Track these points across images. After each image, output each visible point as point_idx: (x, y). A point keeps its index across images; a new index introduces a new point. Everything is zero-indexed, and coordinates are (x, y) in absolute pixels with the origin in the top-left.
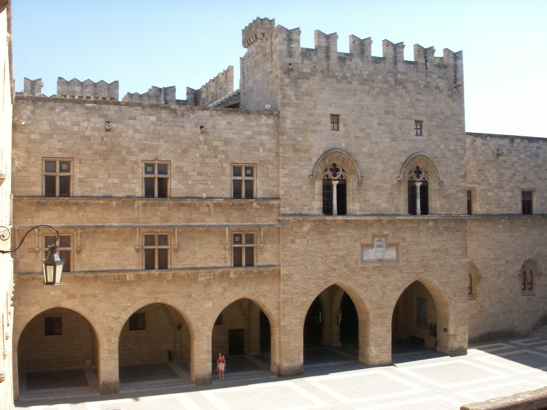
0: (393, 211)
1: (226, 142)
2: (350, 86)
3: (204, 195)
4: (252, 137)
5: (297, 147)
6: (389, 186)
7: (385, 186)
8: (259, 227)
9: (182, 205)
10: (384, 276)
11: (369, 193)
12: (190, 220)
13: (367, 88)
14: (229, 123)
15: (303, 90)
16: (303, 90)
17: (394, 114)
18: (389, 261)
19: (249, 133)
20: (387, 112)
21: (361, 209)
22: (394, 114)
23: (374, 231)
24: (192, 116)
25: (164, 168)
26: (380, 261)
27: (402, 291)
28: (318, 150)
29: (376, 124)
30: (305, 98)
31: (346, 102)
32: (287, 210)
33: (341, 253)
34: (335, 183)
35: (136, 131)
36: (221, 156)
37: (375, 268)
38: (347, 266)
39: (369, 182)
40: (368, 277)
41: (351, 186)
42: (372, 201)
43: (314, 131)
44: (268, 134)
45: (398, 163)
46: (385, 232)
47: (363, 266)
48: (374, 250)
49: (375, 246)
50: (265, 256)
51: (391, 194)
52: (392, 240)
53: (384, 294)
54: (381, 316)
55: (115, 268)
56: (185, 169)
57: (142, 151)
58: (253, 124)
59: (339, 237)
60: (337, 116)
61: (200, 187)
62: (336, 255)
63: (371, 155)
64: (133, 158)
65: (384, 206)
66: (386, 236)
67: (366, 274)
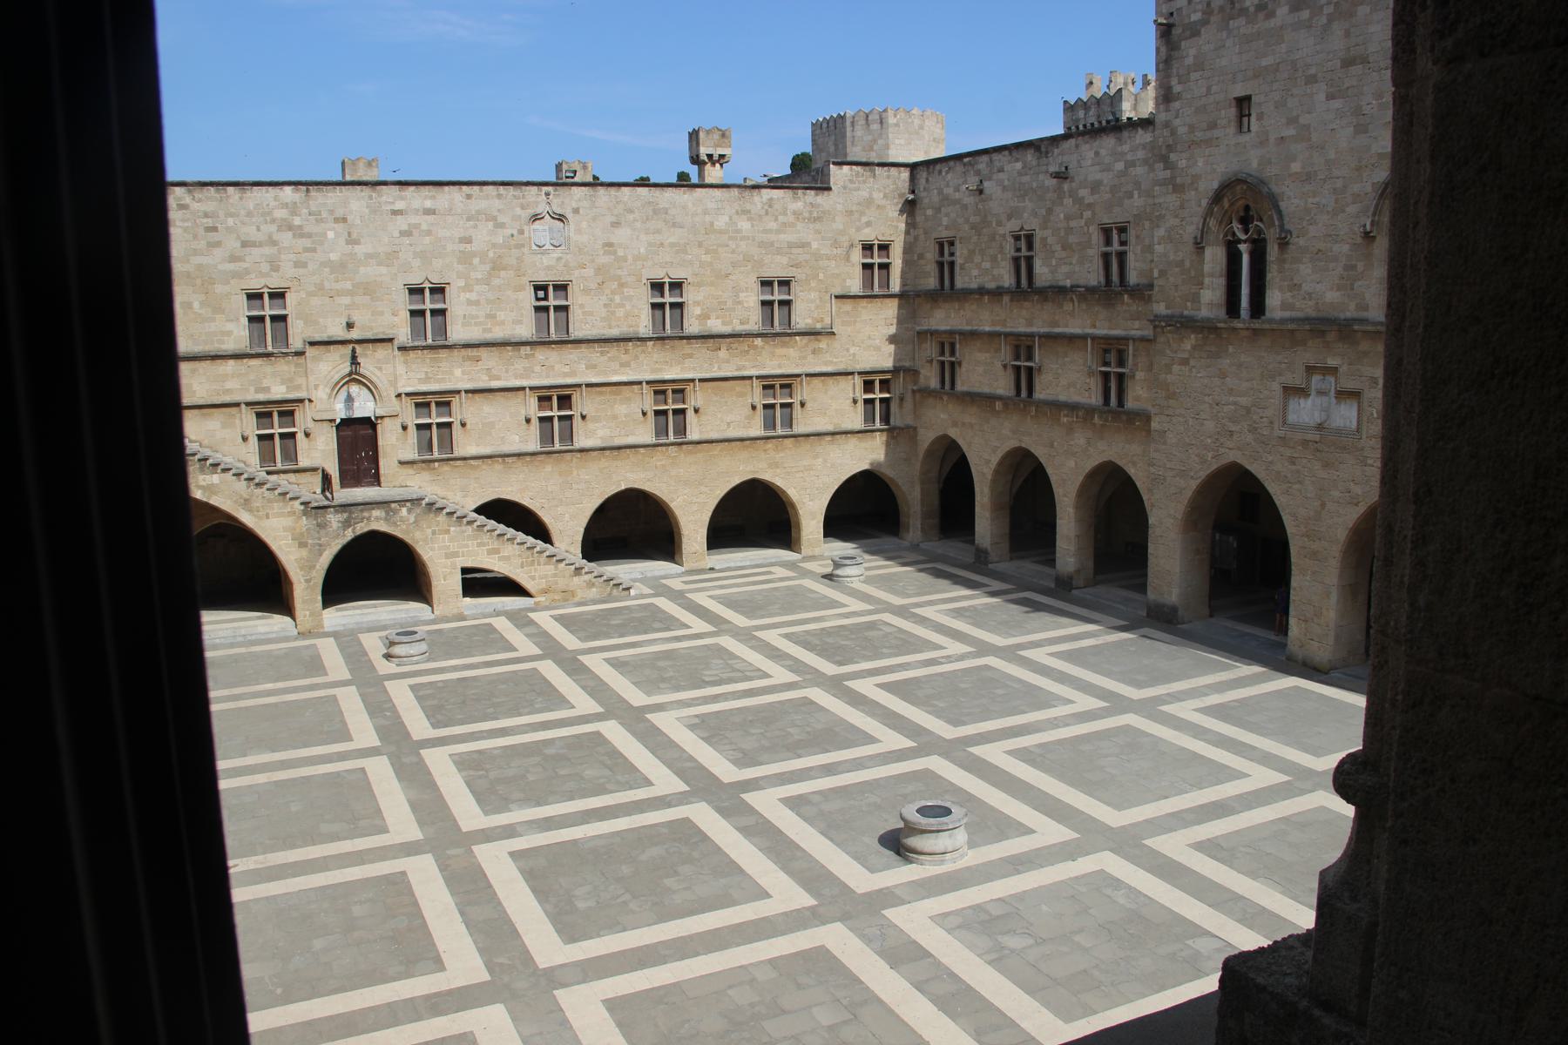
0: (1351, 312)
1: (1095, 187)
2: (1272, 23)
3: (1068, 283)
4: (1124, 173)
5: (1179, 180)
6: (1346, 248)
7: (1336, 248)
8: (1126, 339)
9: (1046, 300)
10: (1326, 465)
11: (1302, 267)
12: (1056, 325)
13: (1305, 14)
14: (1097, 154)
15: (1189, 61)
16: (1189, 61)
17: (1364, 60)
18: (1339, 432)
19: (1120, 166)
20: (1348, 63)
21: (1285, 306)
22: (1364, 60)
23: (1308, 355)
24: (1056, 151)
25: (1030, 239)
26: (1320, 427)
27: (1362, 509)
28: (1211, 184)
29: (1322, 96)
30: (1194, 76)
31: (1264, 62)
32: (1160, 308)
33: (1243, 401)
34: (1243, 247)
35: (1004, 189)
36: (1087, 214)
37: (1305, 443)
38: (1253, 430)
39: (1302, 242)
40: (1292, 461)
41: (1272, 252)
42: (1306, 287)
43: (1208, 142)
44: (1145, 162)
45: (1369, 189)
46: (1332, 362)
47: (1281, 434)
48: (1310, 401)
49: (1313, 393)
50: (1138, 395)
51: (1348, 268)
52: (1350, 385)
53: (1323, 505)
54: (1314, 555)
55: (986, 390)
56: (1050, 240)
57: (1009, 218)
58: (1126, 148)
59: (1240, 365)
60: (1248, 98)
61: (1065, 269)
62: (1235, 404)
63: (1308, 177)
64: (1001, 231)
65: (1332, 296)
66: (1333, 371)
67: (1288, 452)
